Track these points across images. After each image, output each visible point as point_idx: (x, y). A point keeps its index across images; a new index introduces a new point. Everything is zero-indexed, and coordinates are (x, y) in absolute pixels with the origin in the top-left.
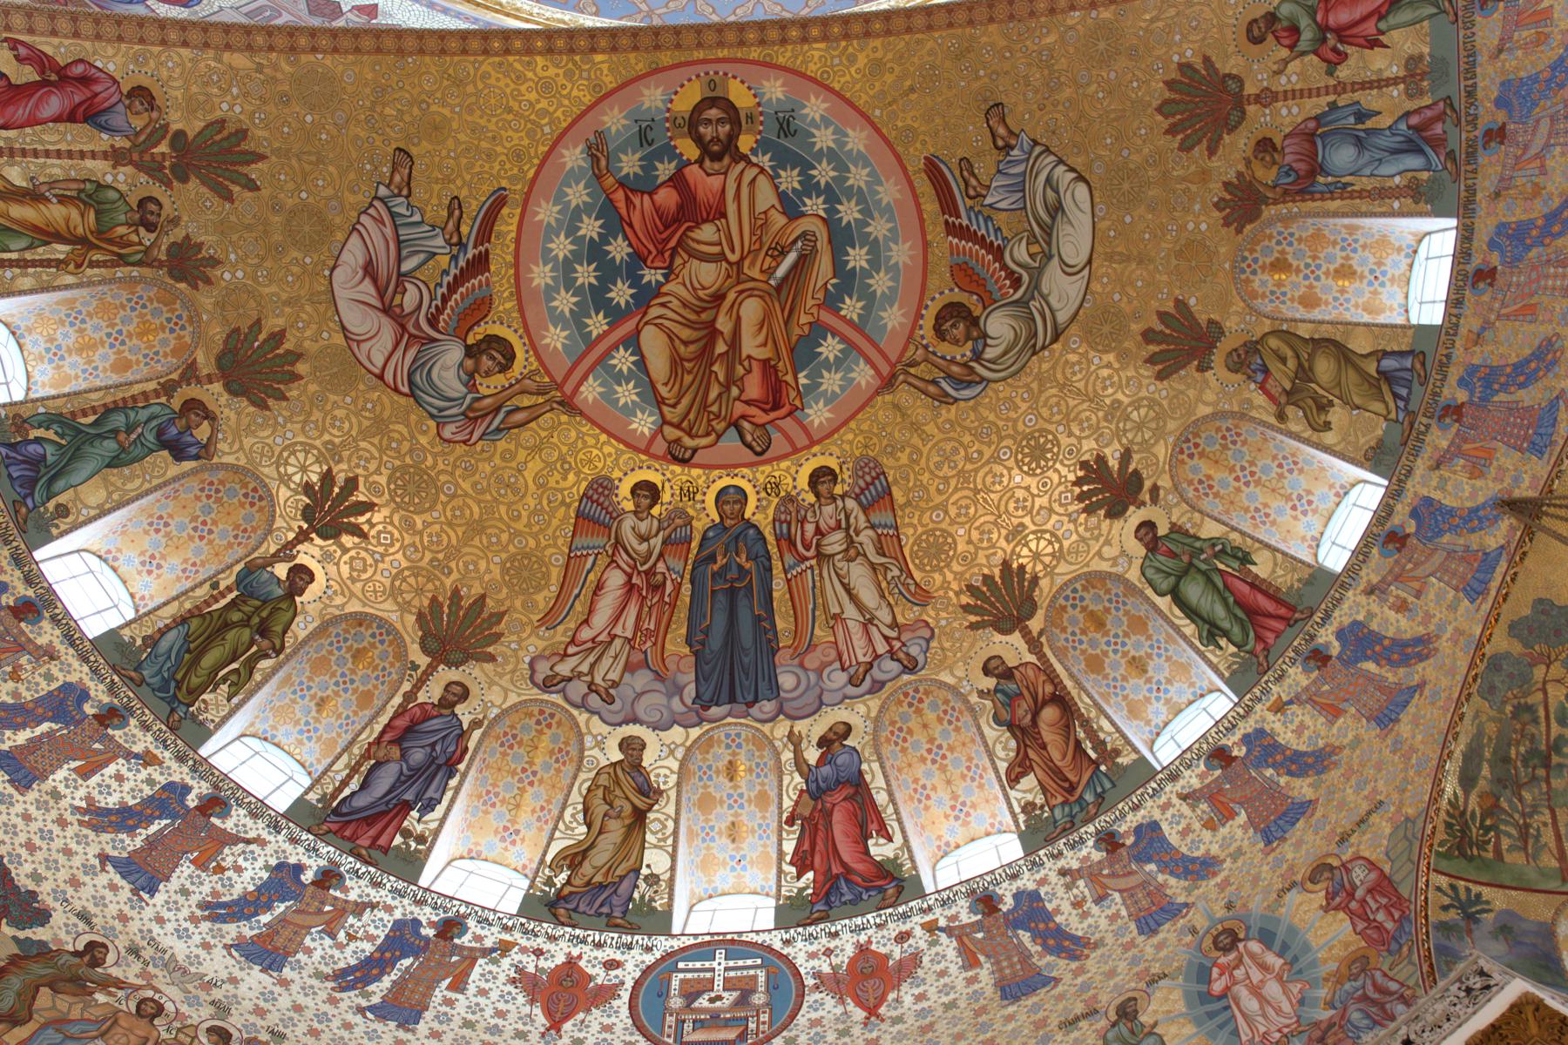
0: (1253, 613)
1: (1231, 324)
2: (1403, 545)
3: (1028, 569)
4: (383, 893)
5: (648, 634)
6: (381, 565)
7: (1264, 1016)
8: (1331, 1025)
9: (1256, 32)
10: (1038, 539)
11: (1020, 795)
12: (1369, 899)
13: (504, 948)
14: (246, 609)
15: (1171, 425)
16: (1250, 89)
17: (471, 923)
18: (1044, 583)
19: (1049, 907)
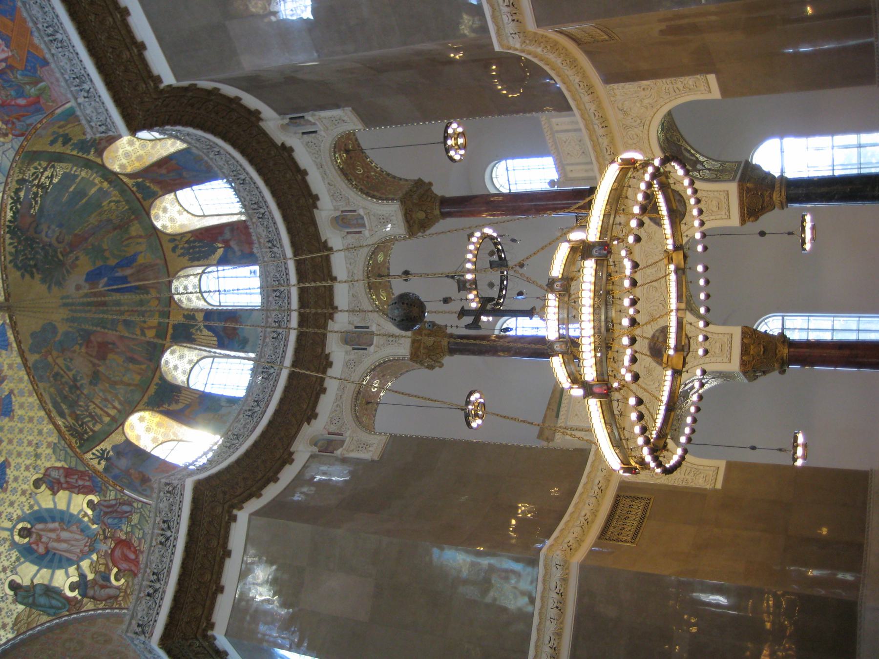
7: (73, 546)
8: (104, 531)
12: (68, 480)
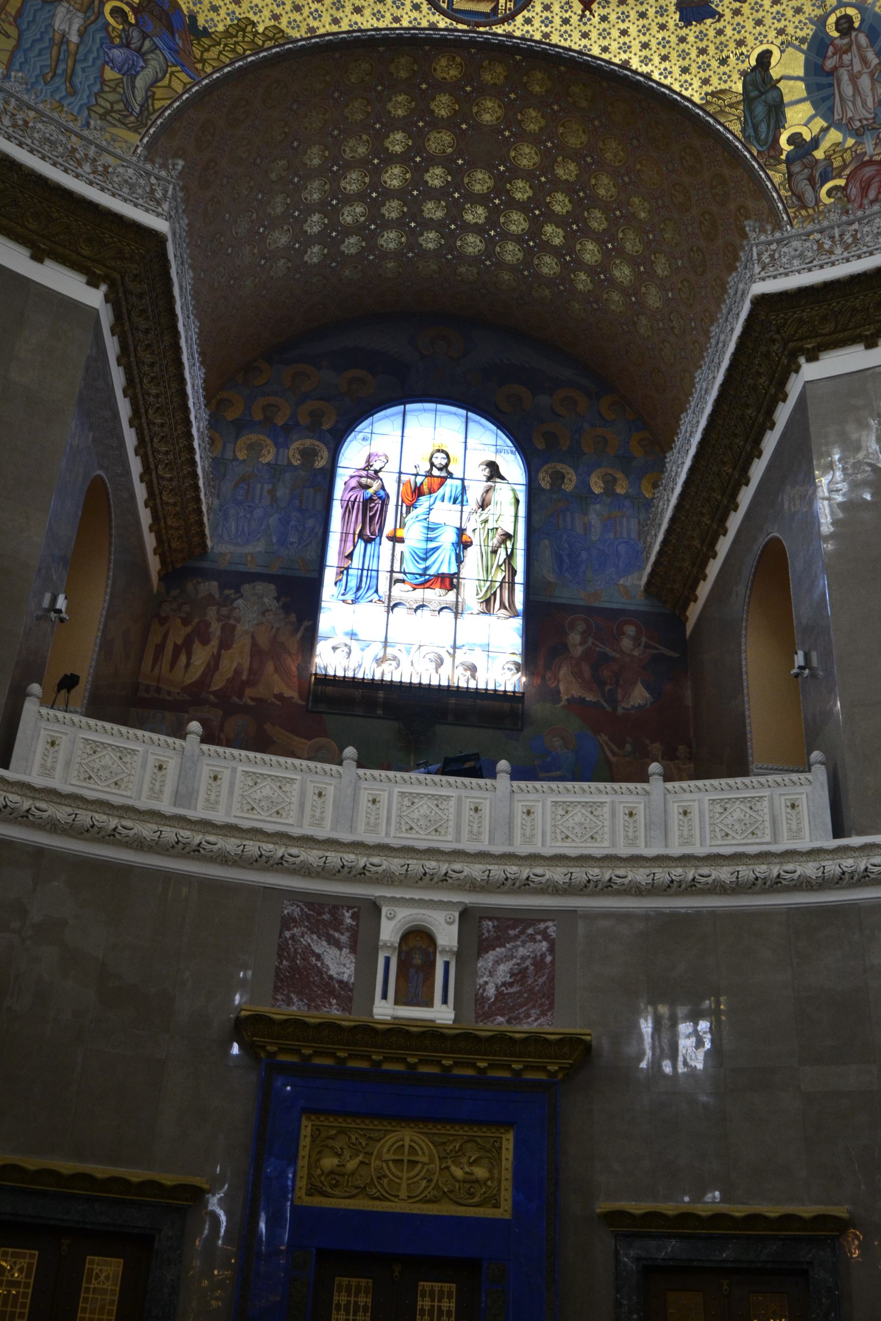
7: (854, 103)
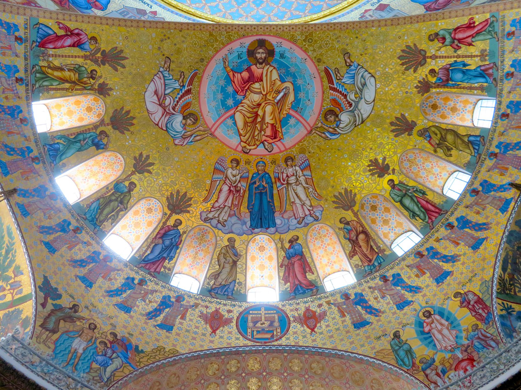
0: (427, 210)
1: (419, 122)
2: (478, 194)
3: (353, 191)
4: (159, 287)
5: (236, 205)
6: (156, 183)
7: (445, 341)
8: (469, 346)
9: (431, 38)
10: (356, 182)
11: (353, 262)
13: (196, 305)
14: (117, 195)
15: (399, 151)
16: (428, 54)
17: (186, 297)
18: (358, 196)
19: (366, 298)
